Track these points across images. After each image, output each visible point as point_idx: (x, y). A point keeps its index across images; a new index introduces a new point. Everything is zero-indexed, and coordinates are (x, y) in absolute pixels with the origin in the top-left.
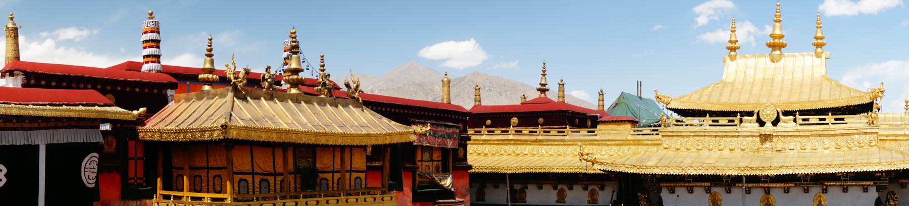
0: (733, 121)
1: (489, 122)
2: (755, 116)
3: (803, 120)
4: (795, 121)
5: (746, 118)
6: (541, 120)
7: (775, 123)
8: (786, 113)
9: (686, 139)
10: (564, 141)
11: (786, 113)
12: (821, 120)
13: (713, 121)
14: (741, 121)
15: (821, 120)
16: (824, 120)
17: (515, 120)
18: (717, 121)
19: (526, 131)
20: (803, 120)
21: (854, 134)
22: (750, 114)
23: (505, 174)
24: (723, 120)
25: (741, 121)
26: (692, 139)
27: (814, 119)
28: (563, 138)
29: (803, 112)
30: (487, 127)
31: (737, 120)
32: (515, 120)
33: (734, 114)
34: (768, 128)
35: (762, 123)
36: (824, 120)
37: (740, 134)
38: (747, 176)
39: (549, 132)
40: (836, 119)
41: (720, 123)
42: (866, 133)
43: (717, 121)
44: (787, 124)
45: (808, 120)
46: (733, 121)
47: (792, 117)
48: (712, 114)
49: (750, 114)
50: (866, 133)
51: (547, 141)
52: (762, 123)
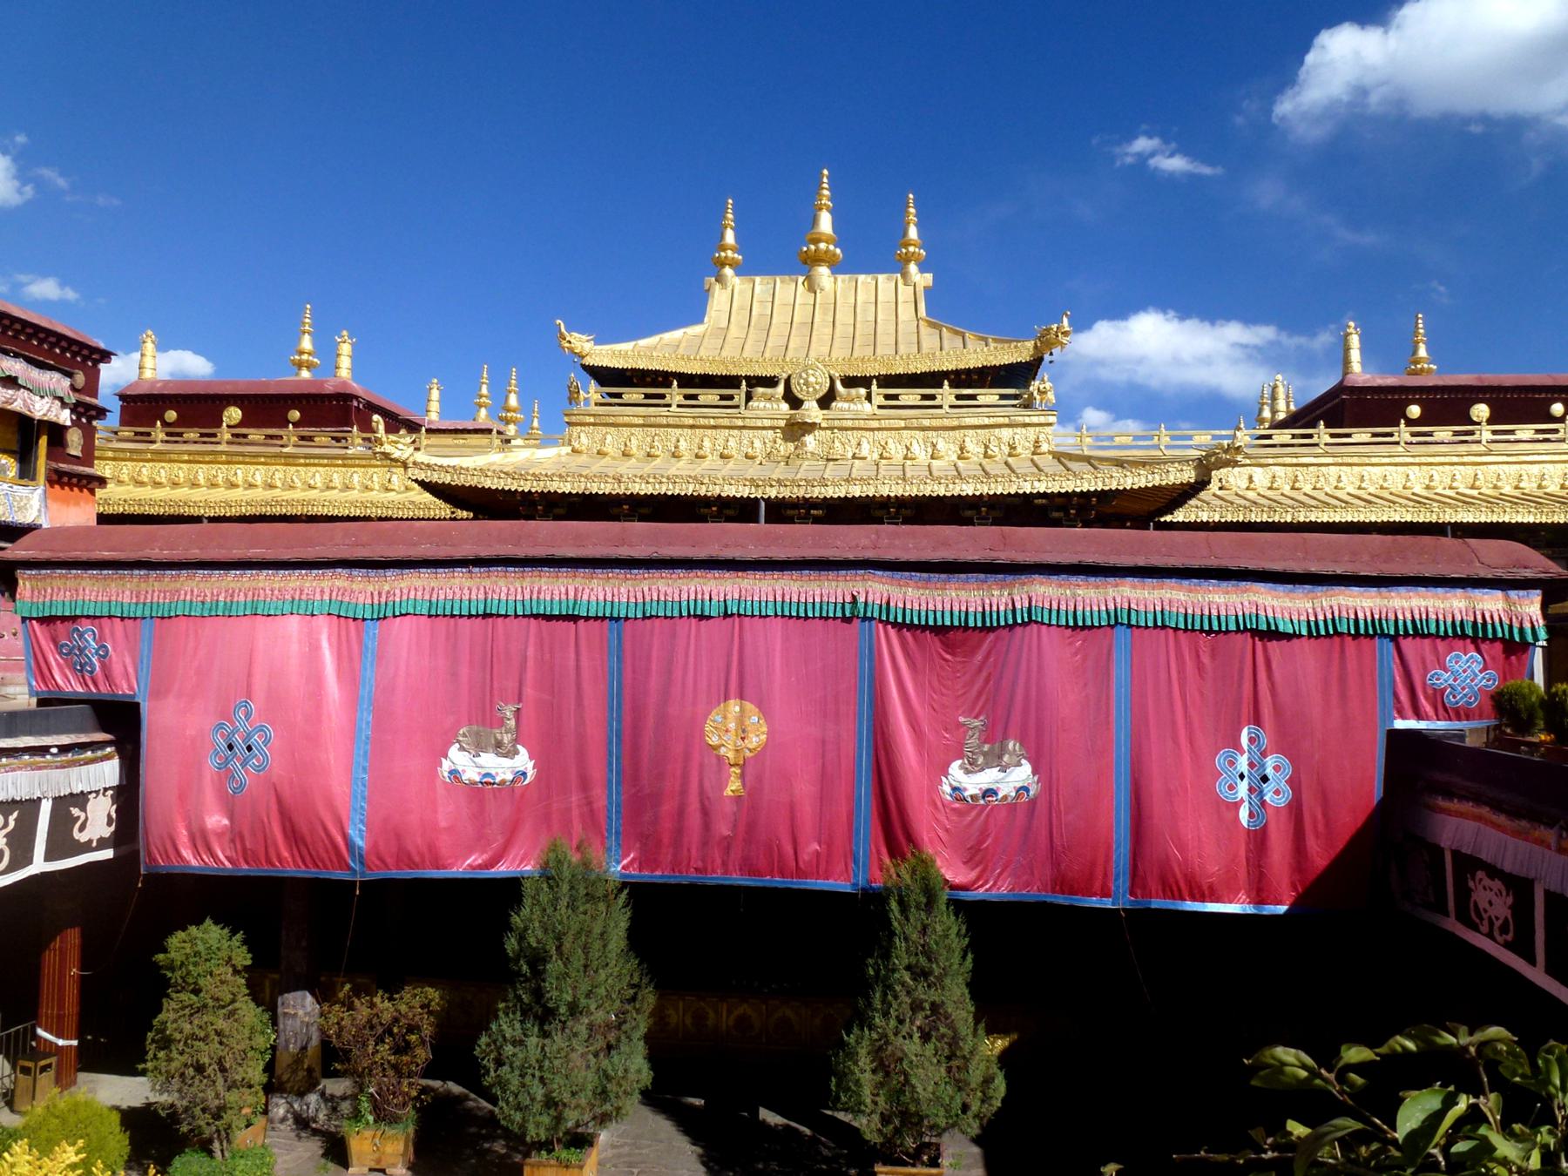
0: (731, 398)
1: (171, 415)
2: (781, 389)
3: (887, 397)
4: (869, 398)
5: (760, 390)
6: (295, 415)
7: (826, 401)
8: (850, 382)
9: (626, 431)
10: (344, 458)
11: (850, 382)
12: (924, 397)
13: (687, 397)
14: (749, 397)
15: (924, 397)
16: (933, 397)
17: (234, 414)
18: (694, 397)
19: (255, 435)
20: (887, 397)
21: (1000, 426)
22: (770, 382)
24: (709, 396)
25: (749, 397)
26: (635, 430)
27: (910, 396)
28: (343, 452)
29: (888, 381)
30: (165, 424)
31: (740, 395)
32: (234, 414)
33: (731, 381)
34: (811, 411)
35: (795, 402)
36: (933, 397)
37: (748, 423)
38: (768, 501)
39: (310, 439)
40: (958, 397)
41: (702, 399)
42: (1025, 425)
43: (694, 397)
44: (854, 405)
45: (895, 397)
46: (731, 398)
47: (863, 391)
48: (687, 380)
49: (770, 382)
50: (1025, 425)
51: (306, 457)
52: (795, 402)
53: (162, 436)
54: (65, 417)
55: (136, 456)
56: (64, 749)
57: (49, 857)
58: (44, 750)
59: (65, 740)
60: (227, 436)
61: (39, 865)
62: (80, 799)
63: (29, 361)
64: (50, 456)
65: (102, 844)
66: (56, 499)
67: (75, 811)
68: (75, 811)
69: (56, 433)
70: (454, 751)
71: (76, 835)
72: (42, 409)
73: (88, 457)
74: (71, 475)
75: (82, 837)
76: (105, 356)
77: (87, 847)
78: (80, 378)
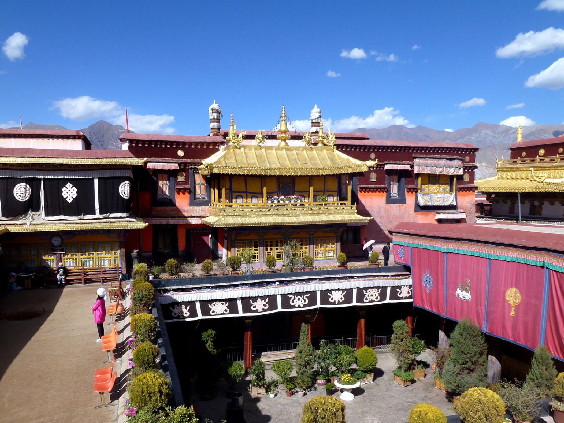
1: (524, 154)
17: (542, 152)
19: (547, 159)
23: (516, 194)
30: (521, 157)
53: (520, 162)
54: (461, 172)
55: (511, 170)
56: (393, 276)
57: (391, 299)
58: (387, 276)
59: (394, 274)
60: (538, 160)
61: (388, 301)
62: (400, 287)
63: (448, 159)
64: (457, 183)
65: (406, 298)
66: (461, 195)
67: (398, 290)
68: (398, 290)
69: (460, 178)
70: (458, 289)
71: (398, 295)
72: (451, 172)
73: (472, 180)
74: (464, 188)
75: (400, 296)
76: (476, 150)
77: (402, 298)
78: (467, 158)
